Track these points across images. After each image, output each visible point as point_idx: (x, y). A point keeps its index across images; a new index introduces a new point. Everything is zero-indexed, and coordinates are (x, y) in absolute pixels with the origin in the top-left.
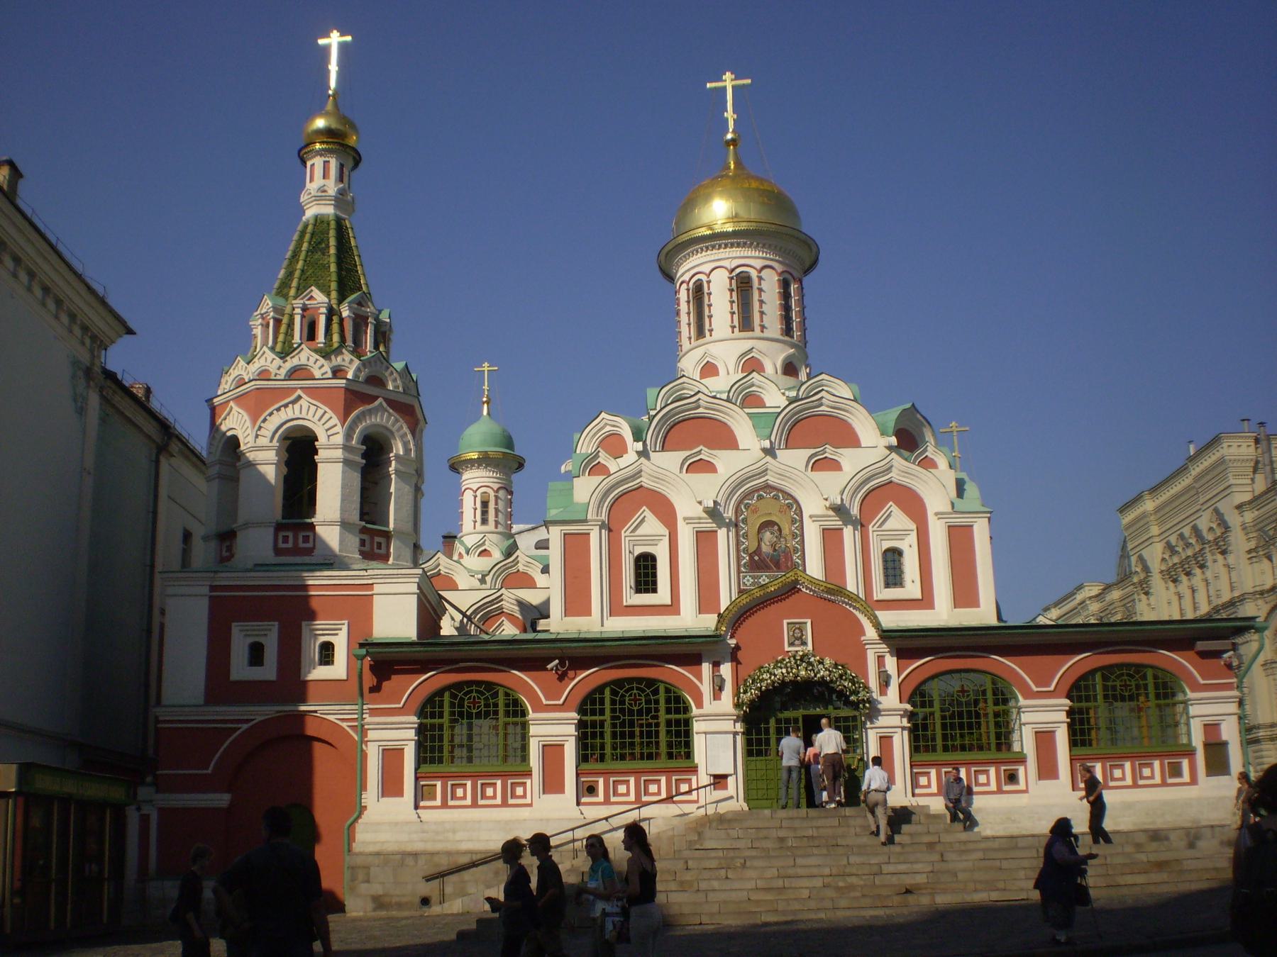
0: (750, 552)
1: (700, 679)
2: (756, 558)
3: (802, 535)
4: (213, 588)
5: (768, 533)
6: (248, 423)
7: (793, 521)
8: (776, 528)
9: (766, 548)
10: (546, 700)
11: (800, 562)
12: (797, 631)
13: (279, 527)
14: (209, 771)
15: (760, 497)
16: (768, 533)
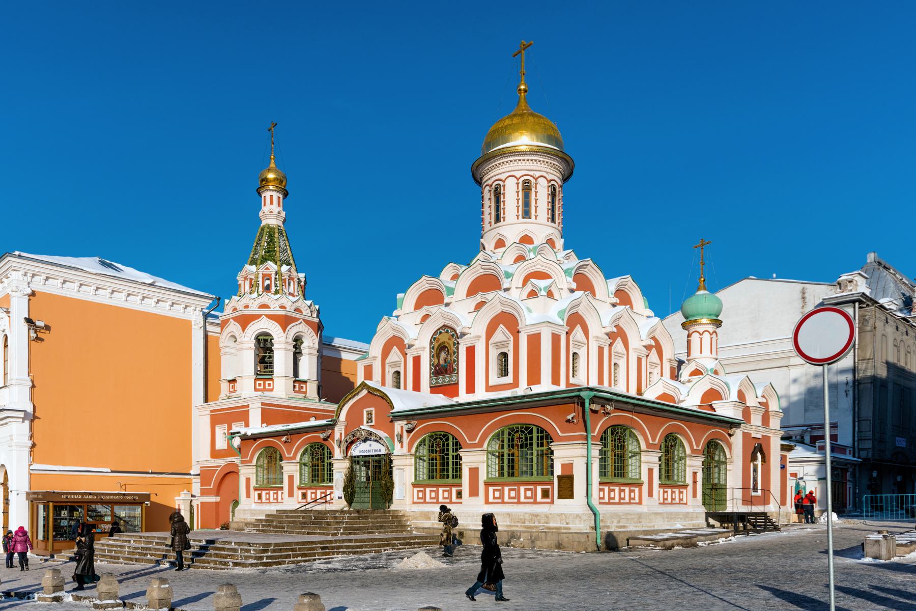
0: (435, 365)
1: (334, 442)
2: (437, 368)
3: (458, 352)
4: (212, 411)
5: (443, 353)
6: (241, 331)
7: (454, 345)
8: (447, 349)
9: (442, 362)
10: (288, 454)
11: (456, 368)
12: (370, 415)
13: (230, 381)
14: (211, 487)
15: (441, 333)
16: (443, 353)
